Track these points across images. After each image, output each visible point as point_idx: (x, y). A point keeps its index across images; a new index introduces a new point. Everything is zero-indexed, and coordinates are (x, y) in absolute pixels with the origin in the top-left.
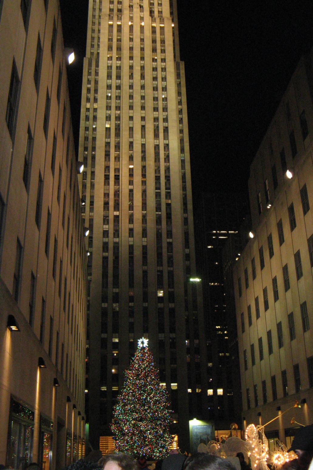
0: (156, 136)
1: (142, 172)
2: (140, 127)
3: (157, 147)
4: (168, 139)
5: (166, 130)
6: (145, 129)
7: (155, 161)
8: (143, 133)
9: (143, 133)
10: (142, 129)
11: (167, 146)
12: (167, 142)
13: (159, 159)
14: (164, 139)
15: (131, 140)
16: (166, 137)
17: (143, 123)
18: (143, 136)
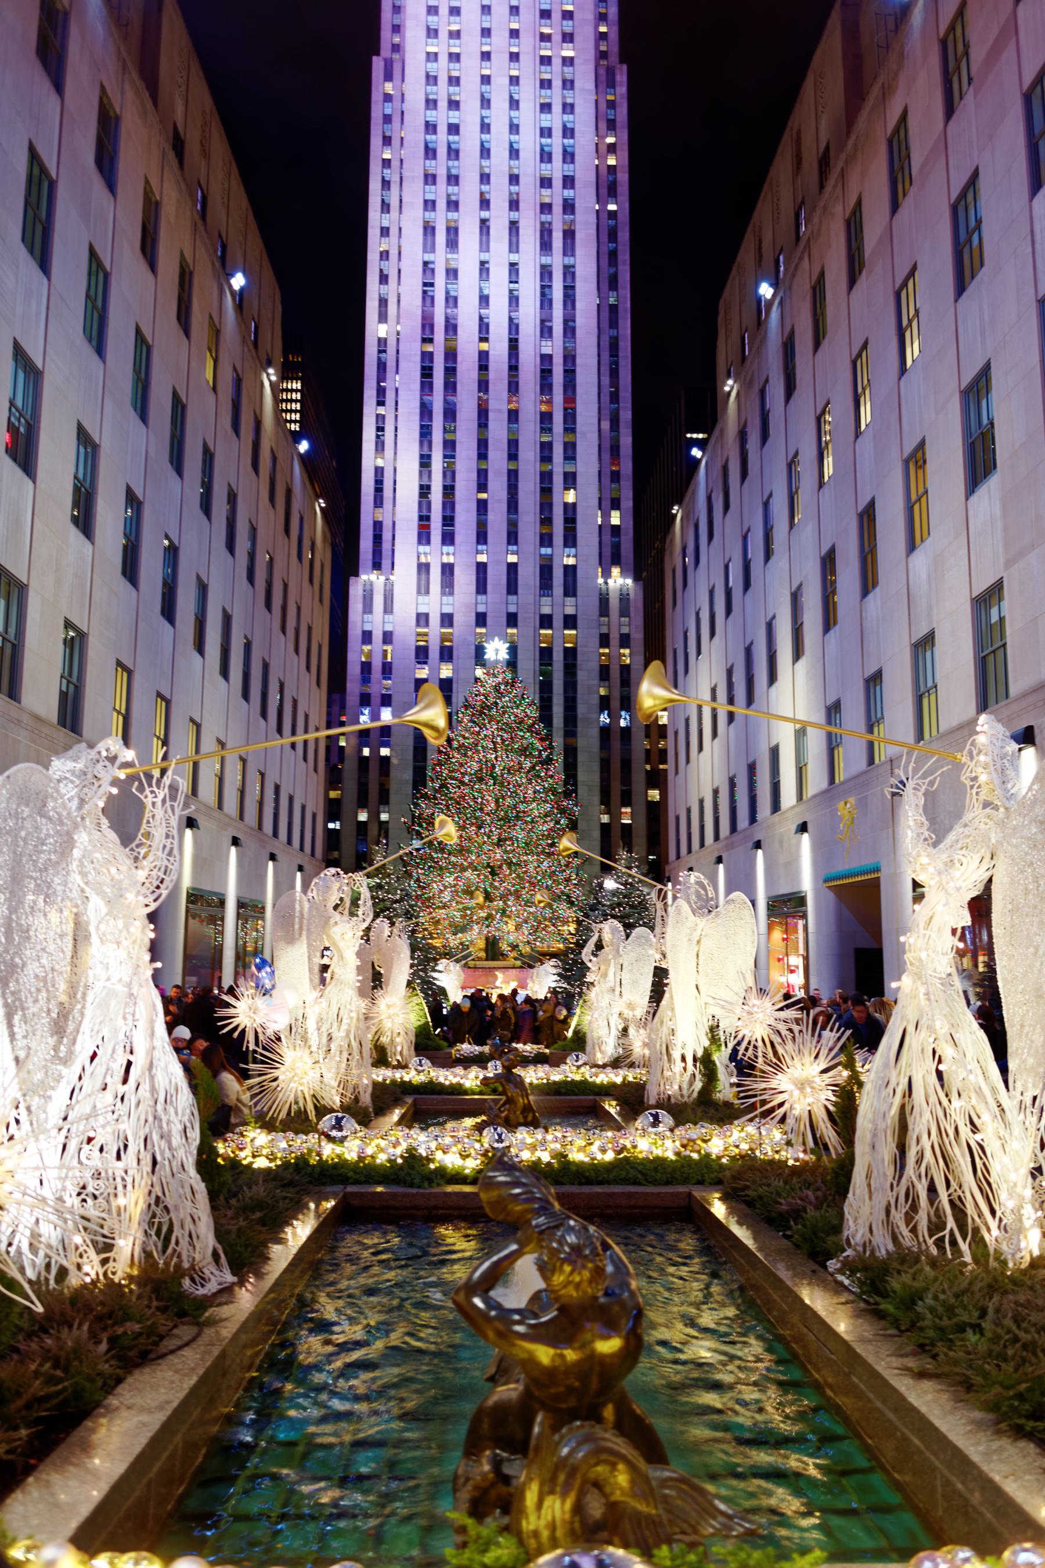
0: (546, 246)
1: (510, 333)
2: (507, 224)
3: (546, 272)
4: (573, 255)
5: (569, 235)
6: (517, 229)
7: (542, 307)
8: (514, 239)
9: (514, 239)
10: (510, 229)
11: (569, 272)
12: (569, 261)
13: (551, 301)
14: (565, 254)
15: (484, 257)
16: (569, 248)
17: (514, 215)
18: (514, 246)
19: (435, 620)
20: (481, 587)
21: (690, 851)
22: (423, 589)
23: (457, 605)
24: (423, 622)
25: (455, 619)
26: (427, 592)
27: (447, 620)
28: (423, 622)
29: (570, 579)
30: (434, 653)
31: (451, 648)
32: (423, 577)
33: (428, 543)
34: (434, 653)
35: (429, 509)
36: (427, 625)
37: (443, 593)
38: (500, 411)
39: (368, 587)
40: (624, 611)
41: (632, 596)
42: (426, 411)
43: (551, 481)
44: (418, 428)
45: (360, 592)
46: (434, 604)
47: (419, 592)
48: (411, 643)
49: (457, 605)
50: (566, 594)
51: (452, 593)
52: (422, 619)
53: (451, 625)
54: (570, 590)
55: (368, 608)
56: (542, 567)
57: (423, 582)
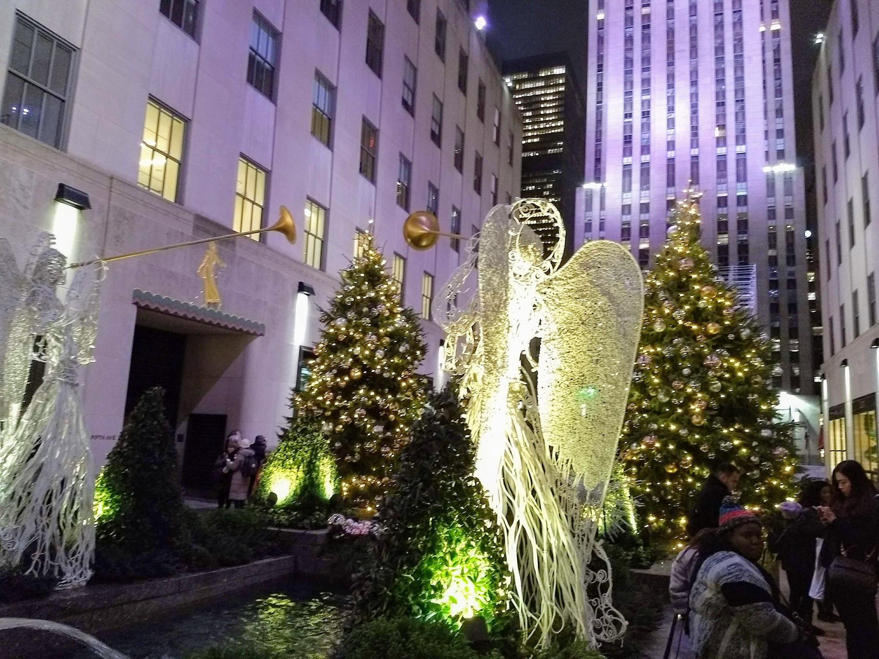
19: (635, 209)
20: (671, 181)
21: (844, 344)
22: (627, 187)
23: (652, 196)
24: (626, 211)
25: (651, 207)
26: (630, 190)
27: (645, 208)
28: (626, 211)
29: (741, 168)
30: (635, 231)
31: (647, 228)
32: (627, 179)
33: (631, 154)
34: (635, 231)
35: (631, 131)
36: (630, 213)
37: (642, 189)
38: (683, 51)
39: (589, 193)
40: (788, 192)
41: (794, 178)
42: (629, 61)
43: (724, 97)
44: (622, 73)
45: (584, 197)
46: (635, 197)
47: (624, 191)
48: (618, 227)
49: (652, 196)
50: (738, 180)
51: (648, 189)
52: (626, 209)
53: (648, 211)
54: (741, 177)
55: (589, 207)
56: (718, 163)
57: (627, 183)
